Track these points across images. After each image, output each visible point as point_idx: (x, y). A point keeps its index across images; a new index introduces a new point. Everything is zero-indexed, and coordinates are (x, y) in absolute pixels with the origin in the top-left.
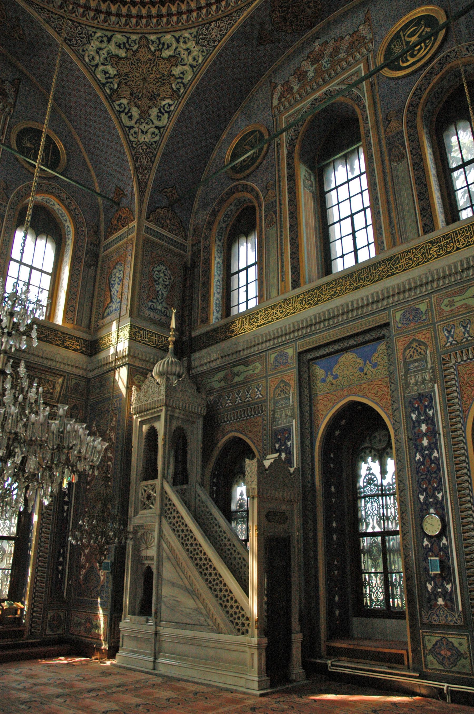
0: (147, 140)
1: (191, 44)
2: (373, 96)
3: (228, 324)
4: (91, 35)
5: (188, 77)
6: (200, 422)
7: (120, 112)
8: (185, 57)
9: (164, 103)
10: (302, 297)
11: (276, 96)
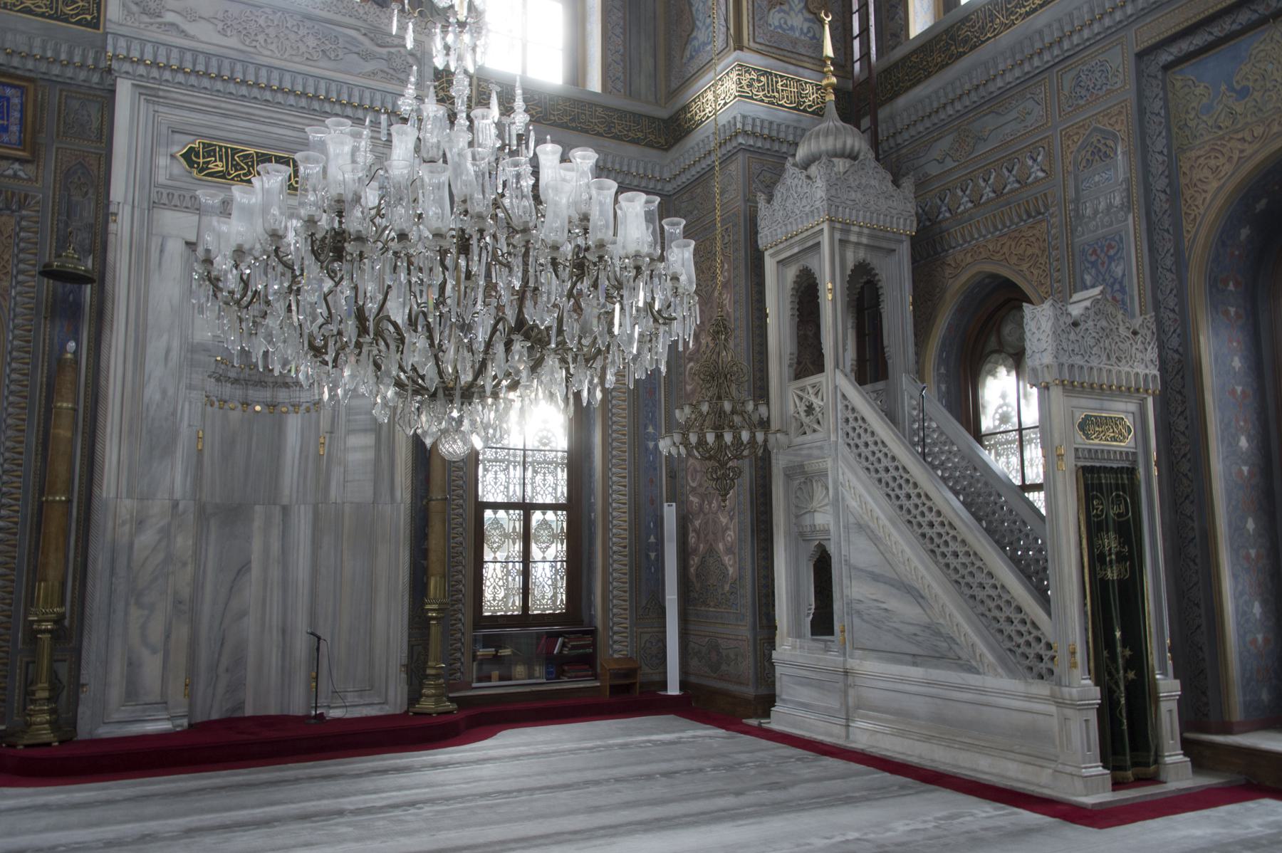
3: (952, 26)
6: (905, 250)
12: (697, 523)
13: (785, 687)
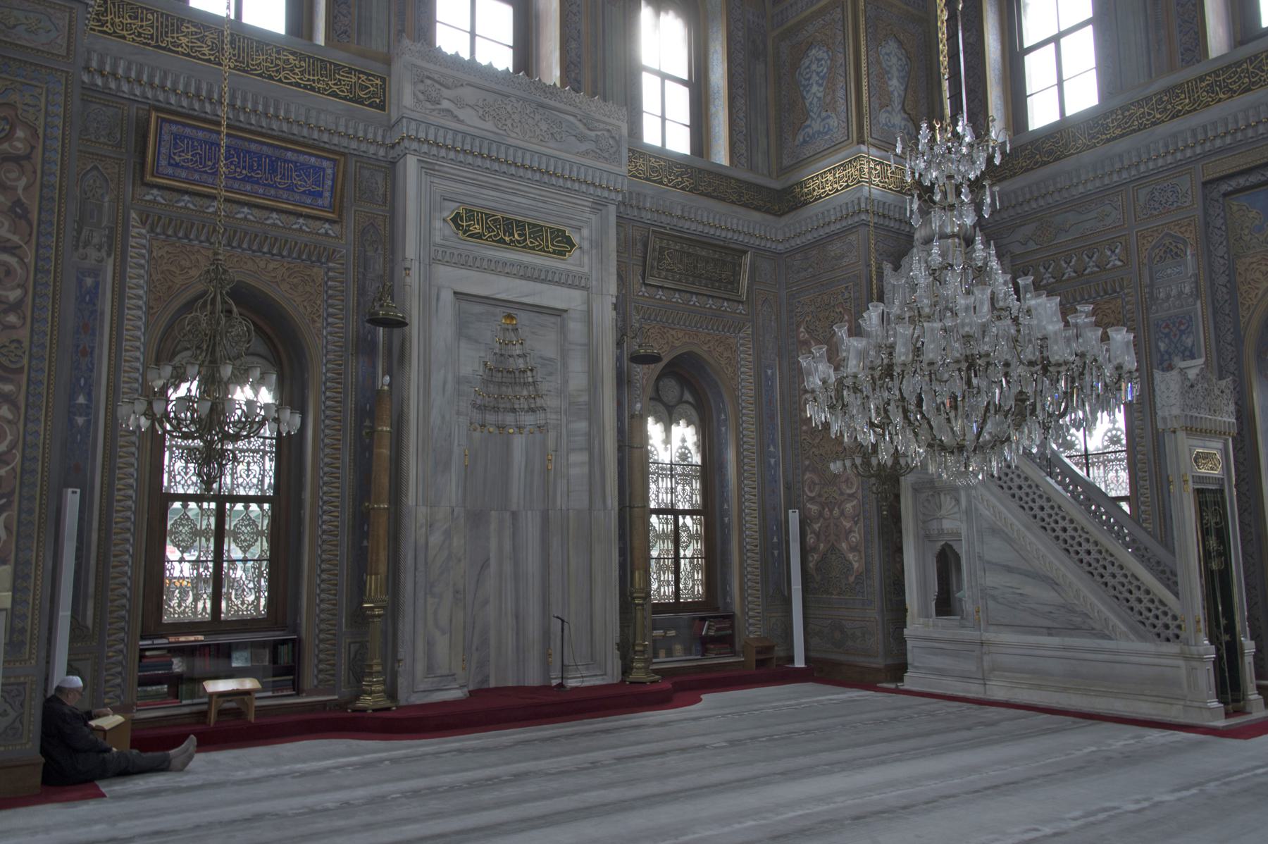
10: (1209, 80)
12: (816, 527)
13: (914, 654)
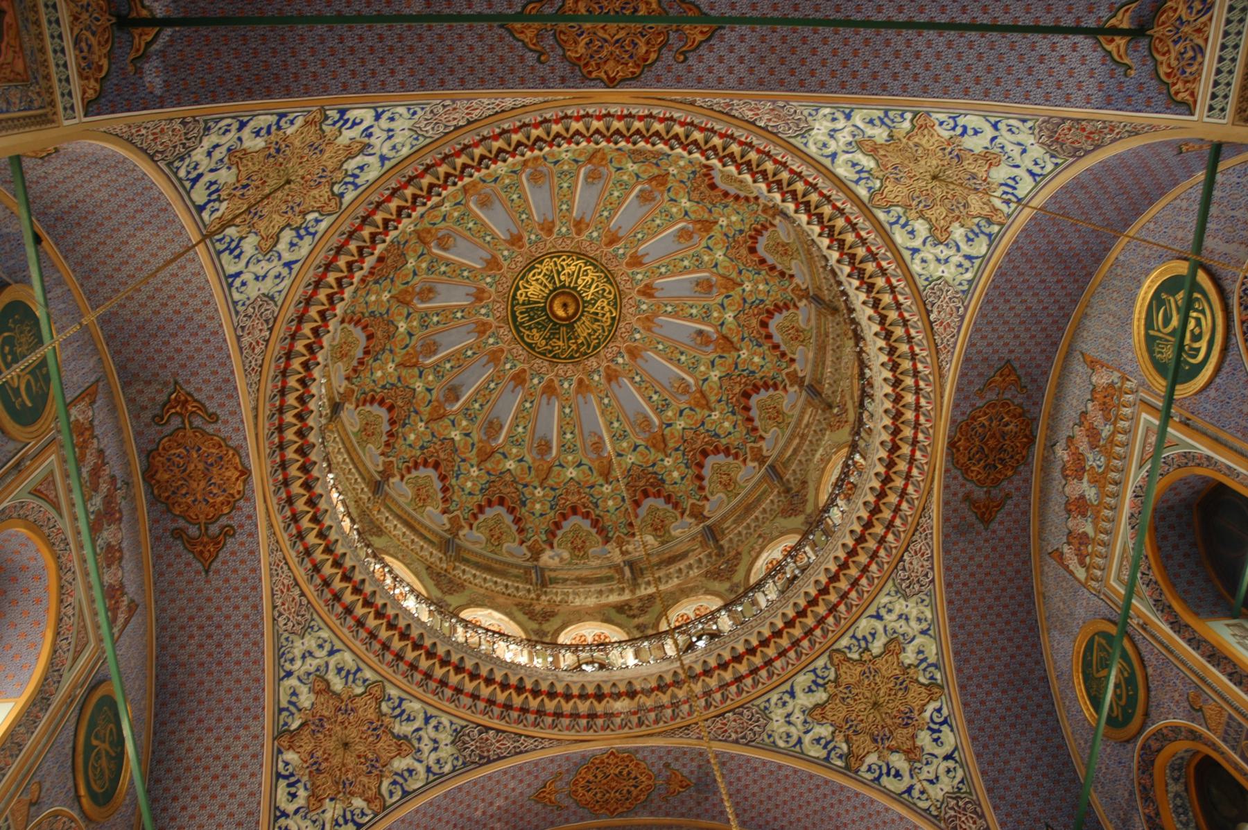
0: (947, 789)
1: (900, 606)
2: (1205, 434)
4: (766, 708)
5: (932, 651)
7: (877, 779)
8: (905, 629)
9: (927, 715)
11: (1073, 564)
